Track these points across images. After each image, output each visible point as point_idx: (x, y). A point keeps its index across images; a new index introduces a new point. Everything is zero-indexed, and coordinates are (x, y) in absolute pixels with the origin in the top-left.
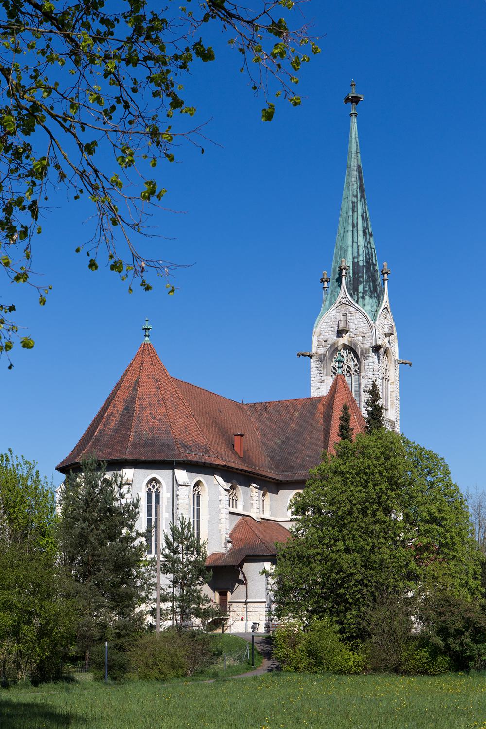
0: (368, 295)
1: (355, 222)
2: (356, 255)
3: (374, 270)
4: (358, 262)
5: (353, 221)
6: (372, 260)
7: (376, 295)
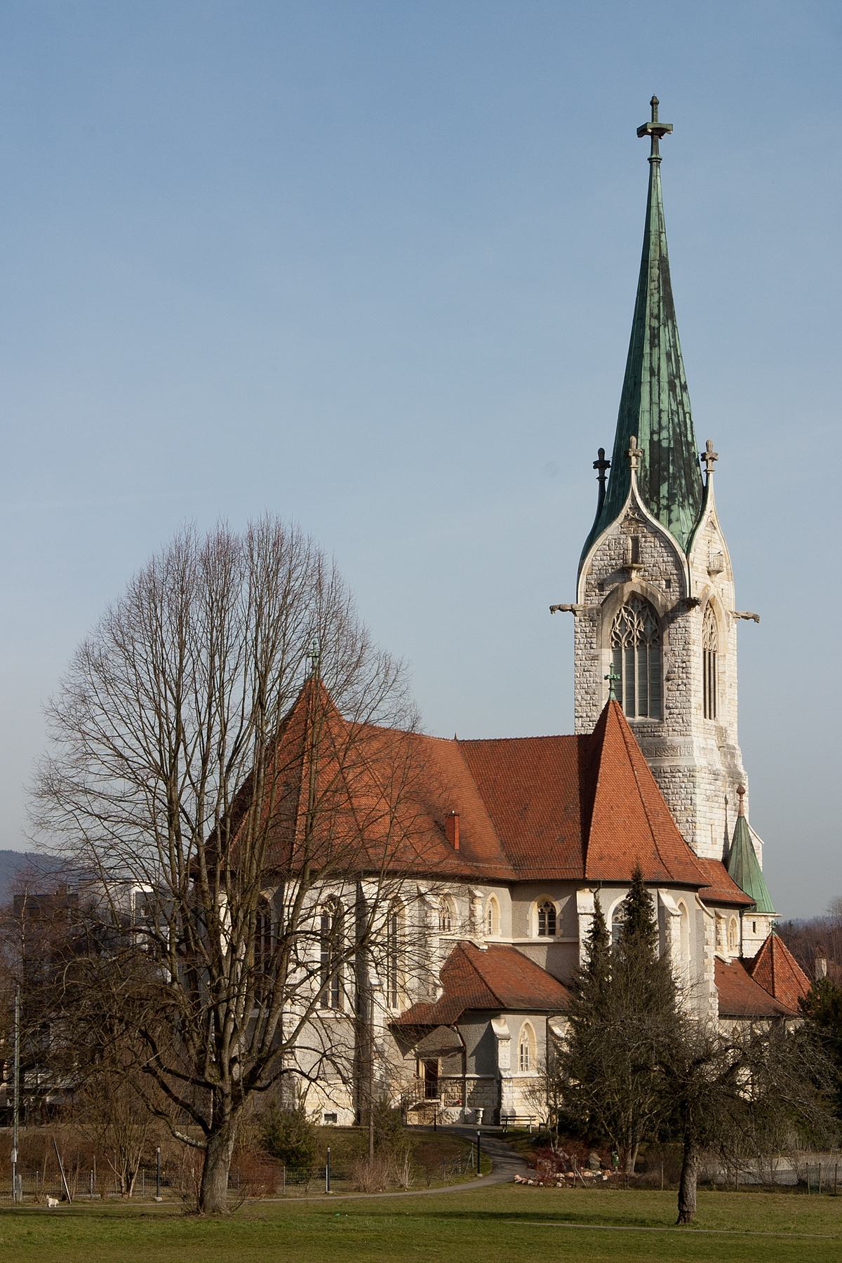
0: (677, 502)
1: (655, 365)
2: (656, 427)
3: (689, 453)
4: (659, 441)
5: (651, 364)
6: (686, 436)
7: (691, 501)
